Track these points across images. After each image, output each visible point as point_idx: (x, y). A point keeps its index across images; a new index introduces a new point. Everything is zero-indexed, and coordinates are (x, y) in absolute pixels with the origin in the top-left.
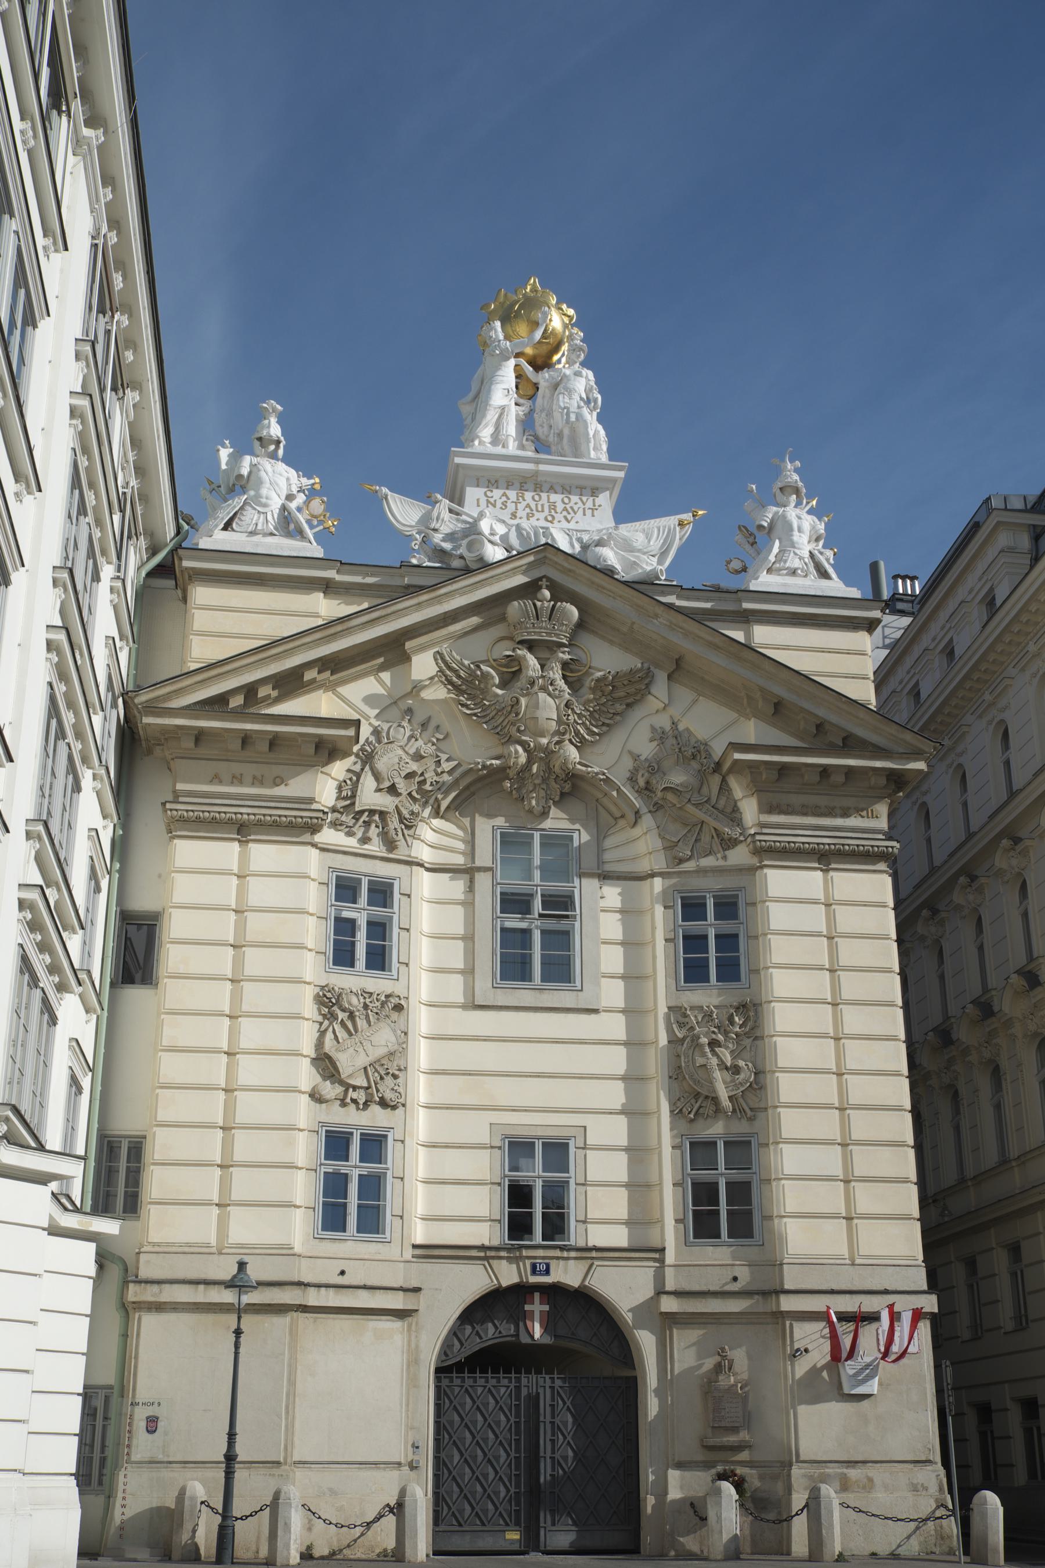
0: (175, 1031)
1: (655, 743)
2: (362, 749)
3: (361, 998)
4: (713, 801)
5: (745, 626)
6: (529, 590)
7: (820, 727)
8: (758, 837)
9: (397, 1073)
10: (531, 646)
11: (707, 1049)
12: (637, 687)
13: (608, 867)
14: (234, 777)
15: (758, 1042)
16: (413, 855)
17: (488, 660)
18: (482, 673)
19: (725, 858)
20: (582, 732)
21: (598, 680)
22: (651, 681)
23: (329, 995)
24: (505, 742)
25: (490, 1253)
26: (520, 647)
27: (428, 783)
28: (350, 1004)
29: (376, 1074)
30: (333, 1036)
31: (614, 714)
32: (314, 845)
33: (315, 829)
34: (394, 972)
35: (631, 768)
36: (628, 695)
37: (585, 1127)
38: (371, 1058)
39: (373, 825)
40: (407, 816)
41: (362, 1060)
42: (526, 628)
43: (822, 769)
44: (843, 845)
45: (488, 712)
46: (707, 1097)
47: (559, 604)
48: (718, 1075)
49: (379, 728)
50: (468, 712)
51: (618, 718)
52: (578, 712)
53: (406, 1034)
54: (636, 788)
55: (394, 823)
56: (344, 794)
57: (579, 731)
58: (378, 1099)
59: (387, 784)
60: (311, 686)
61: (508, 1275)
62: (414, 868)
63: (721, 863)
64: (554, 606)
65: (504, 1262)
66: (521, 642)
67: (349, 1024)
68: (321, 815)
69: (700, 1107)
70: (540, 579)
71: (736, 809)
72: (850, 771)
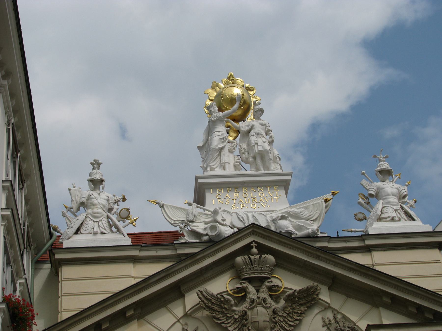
5: (369, 254)
6: (246, 250)
7: (420, 308)
10: (250, 280)
12: (312, 297)
17: (227, 291)
18: (225, 299)
20: (284, 326)
22: (319, 293)
31: (301, 313)
36: (308, 302)
42: (247, 271)
45: (229, 321)
50: (219, 322)
52: (281, 314)
57: (282, 325)
64: (260, 257)
66: (245, 279)
70: (251, 243)
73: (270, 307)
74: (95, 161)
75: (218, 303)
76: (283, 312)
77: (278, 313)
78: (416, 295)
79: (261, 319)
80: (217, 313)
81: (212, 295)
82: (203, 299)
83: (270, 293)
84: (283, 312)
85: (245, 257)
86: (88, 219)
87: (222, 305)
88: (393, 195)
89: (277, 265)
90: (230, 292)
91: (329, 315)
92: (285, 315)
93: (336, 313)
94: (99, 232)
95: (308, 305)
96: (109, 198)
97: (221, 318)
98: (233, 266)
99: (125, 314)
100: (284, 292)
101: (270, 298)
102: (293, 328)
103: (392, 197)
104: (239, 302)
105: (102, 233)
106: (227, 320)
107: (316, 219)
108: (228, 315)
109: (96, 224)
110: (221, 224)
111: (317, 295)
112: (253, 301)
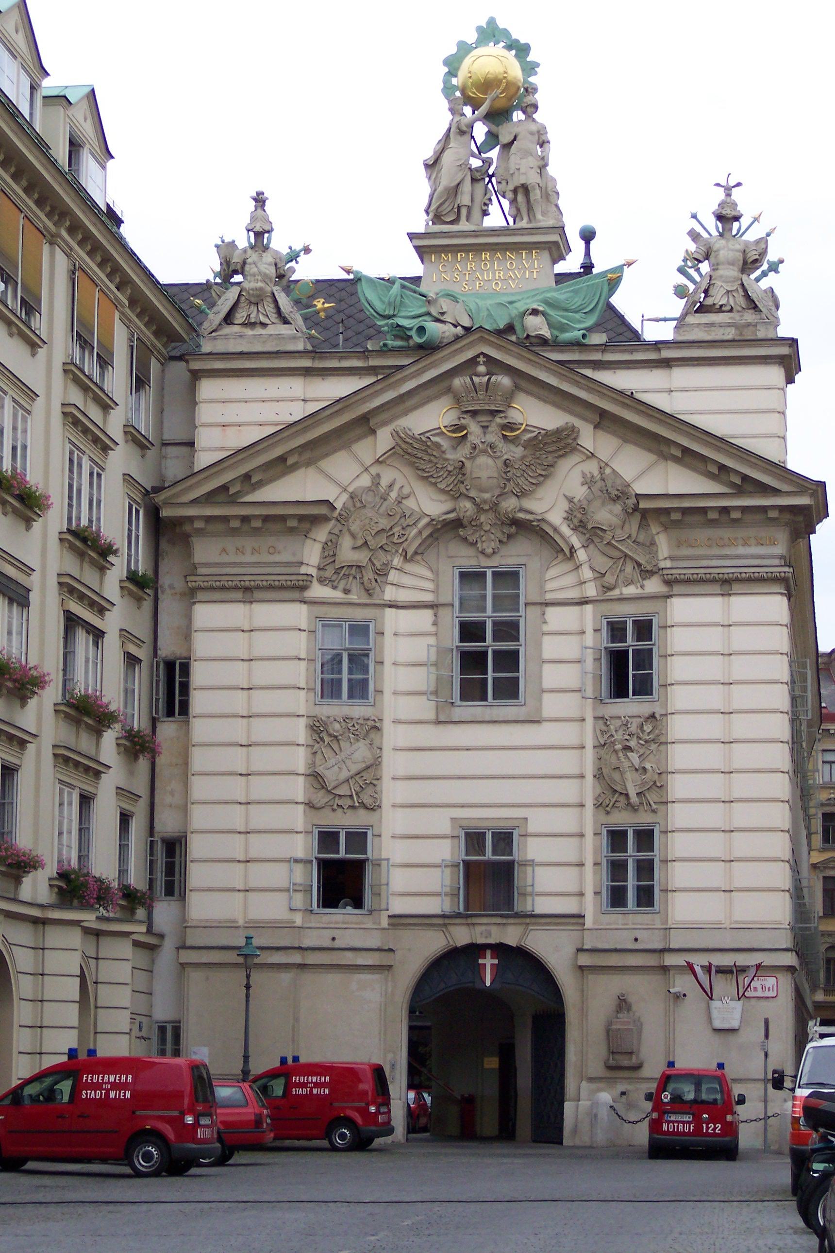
0: (199, 760)
1: (586, 487)
2: (340, 514)
3: (344, 724)
4: (634, 535)
7: (722, 468)
8: (665, 572)
9: (374, 782)
10: (474, 413)
11: (621, 754)
13: (549, 597)
14: (237, 549)
15: (662, 748)
16: (385, 598)
19: (642, 587)
20: (521, 484)
21: (530, 440)
23: (317, 724)
24: (458, 497)
25: (447, 921)
26: (465, 416)
27: (396, 536)
28: (334, 731)
29: (357, 785)
30: (321, 757)
32: (301, 601)
33: (303, 588)
34: (371, 700)
35: (567, 509)
37: (527, 819)
38: (352, 772)
39: (351, 578)
40: (379, 567)
41: (344, 774)
43: (720, 509)
44: (741, 573)
46: (621, 793)
47: (493, 379)
48: (630, 776)
49: (353, 496)
50: (426, 475)
51: (552, 469)
53: (381, 749)
54: (572, 526)
55: (369, 575)
56: (326, 553)
58: (357, 804)
59: (360, 542)
60: (294, 467)
61: (462, 936)
62: (388, 611)
63: (639, 591)
64: (489, 379)
65: (458, 928)
67: (335, 746)
68: (305, 577)
69: (616, 801)
70: (478, 356)
71: (653, 543)
72: (744, 509)
73: (499, 457)
74: (259, 194)
75: (423, 448)
76: (521, 463)
77: (512, 465)
78: (718, 449)
79: (484, 474)
80: (422, 462)
81: (413, 437)
82: (400, 443)
83: (504, 433)
84: (521, 463)
85: (465, 379)
86: (243, 299)
87: (429, 451)
88: (732, 264)
89: (517, 387)
90: (444, 430)
91: (592, 467)
92: (524, 467)
93: (603, 465)
94: (258, 322)
95: (560, 453)
96: (278, 261)
97: (427, 470)
98: (449, 390)
99: (286, 460)
100: (525, 430)
101: (503, 441)
102: (534, 487)
103: (728, 266)
104: (459, 444)
105: (264, 325)
106: (437, 472)
107: (591, 310)
108: (437, 466)
109: (253, 309)
110: (438, 320)
111: (575, 439)
112: (475, 448)
